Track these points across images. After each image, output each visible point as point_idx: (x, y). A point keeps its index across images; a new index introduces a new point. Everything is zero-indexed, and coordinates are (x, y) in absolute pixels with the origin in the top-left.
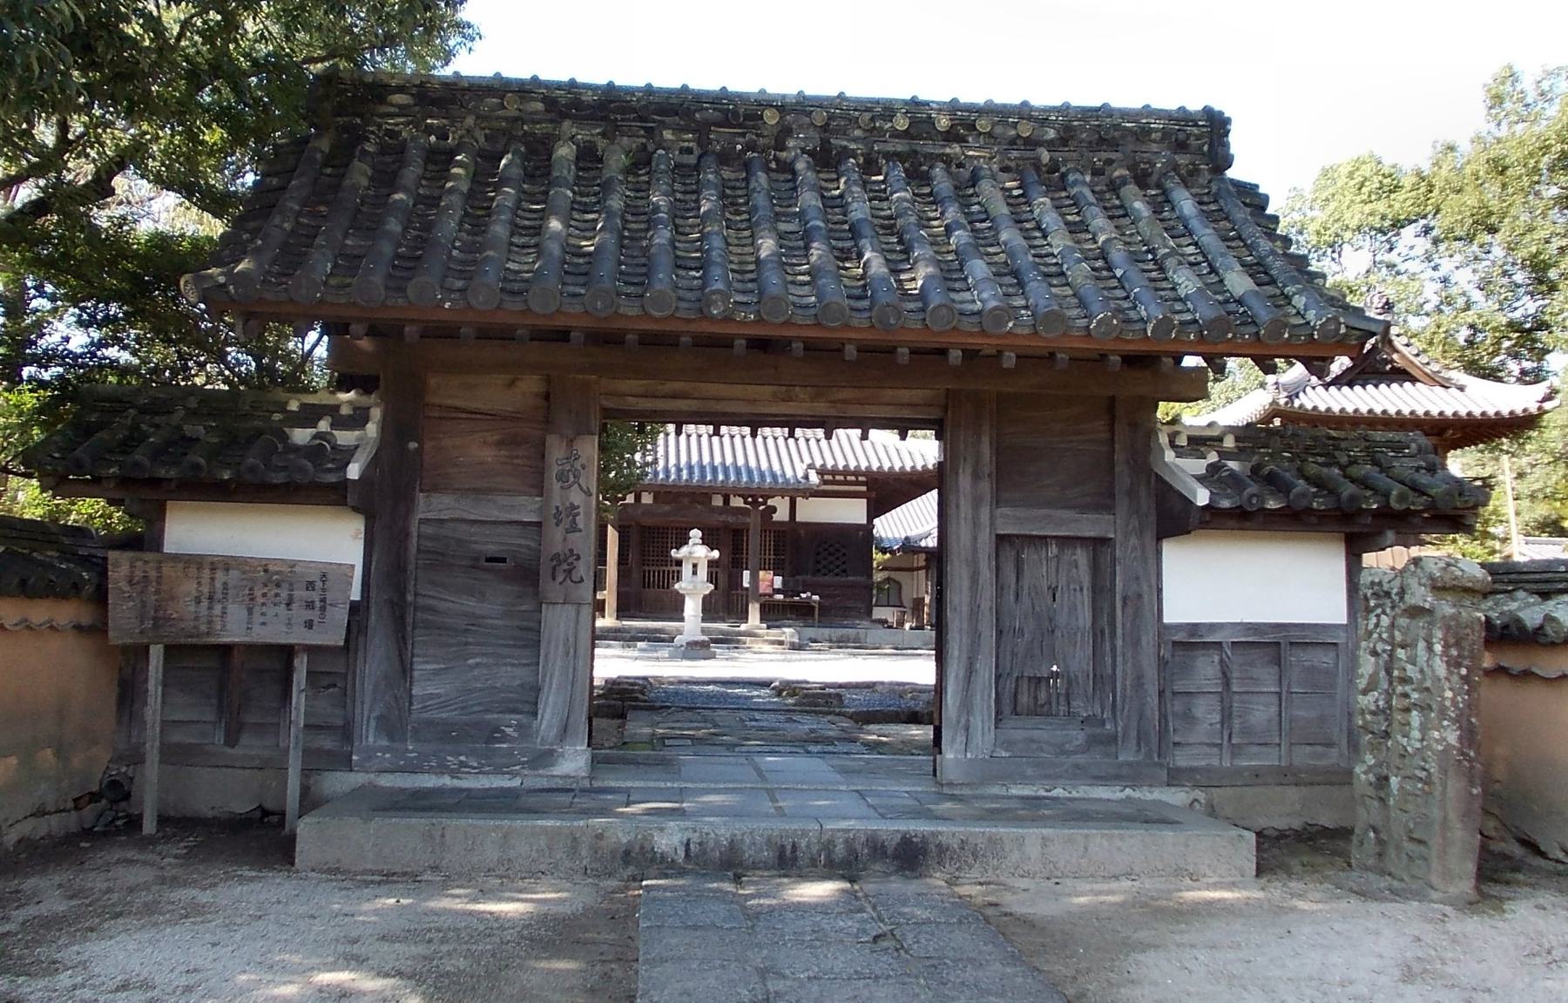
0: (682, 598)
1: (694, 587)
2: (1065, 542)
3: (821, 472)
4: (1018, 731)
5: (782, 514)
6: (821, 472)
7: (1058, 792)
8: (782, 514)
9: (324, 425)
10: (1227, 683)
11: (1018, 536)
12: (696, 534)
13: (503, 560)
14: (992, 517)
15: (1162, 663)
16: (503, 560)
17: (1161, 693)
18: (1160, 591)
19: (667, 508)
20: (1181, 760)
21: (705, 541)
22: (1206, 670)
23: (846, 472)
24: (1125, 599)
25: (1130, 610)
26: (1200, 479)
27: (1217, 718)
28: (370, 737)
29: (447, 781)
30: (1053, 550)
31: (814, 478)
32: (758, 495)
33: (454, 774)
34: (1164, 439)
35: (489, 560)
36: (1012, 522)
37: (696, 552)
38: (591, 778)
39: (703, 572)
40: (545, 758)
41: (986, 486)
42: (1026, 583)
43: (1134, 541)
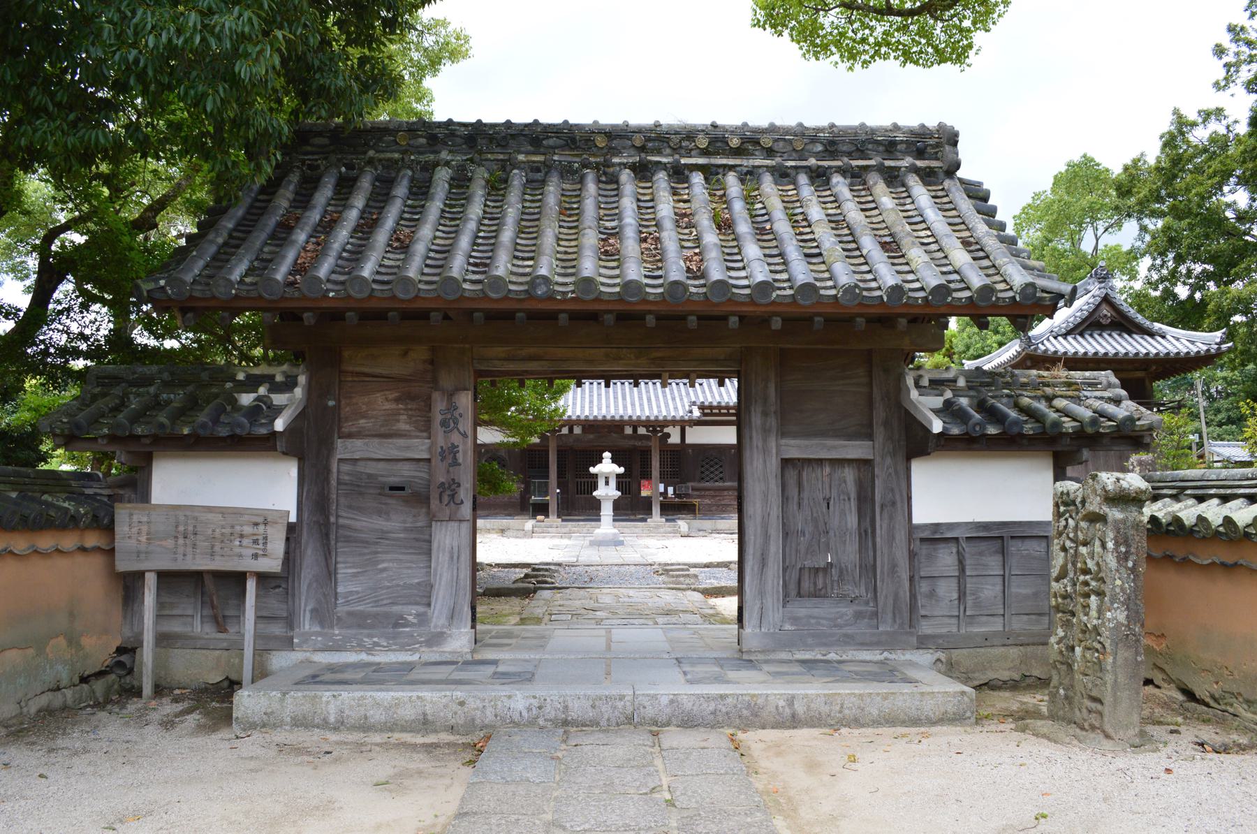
1: (607, 492)
2: (834, 462)
3: (702, 407)
5: (675, 439)
6: (702, 407)
7: (832, 656)
8: (675, 439)
9: (262, 390)
10: (962, 569)
11: (799, 459)
12: (607, 455)
13: (402, 489)
14: (778, 446)
15: (912, 555)
16: (402, 489)
17: (911, 579)
18: (909, 498)
19: (591, 436)
20: (926, 628)
21: (614, 460)
22: (946, 560)
23: (719, 407)
24: (882, 506)
25: (886, 515)
26: (937, 412)
27: (955, 596)
28: (307, 624)
29: (364, 657)
30: (827, 470)
31: (697, 413)
32: (657, 426)
33: (369, 651)
34: (910, 381)
35: (392, 488)
36: (796, 448)
37: (607, 467)
38: (473, 652)
39: (613, 483)
40: (436, 639)
41: (773, 422)
42: (805, 495)
43: (888, 461)
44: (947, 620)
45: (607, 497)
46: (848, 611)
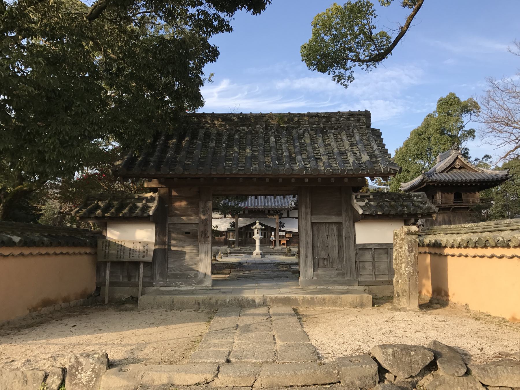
2: (329, 223)
7: (330, 287)
9: (144, 202)
10: (374, 259)
11: (318, 223)
13: (189, 233)
14: (311, 219)
15: (356, 254)
16: (189, 233)
17: (356, 262)
18: (355, 235)
20: (362, 279)
22: (368, 256)
24: (345, 238)
25: (347, 240)
26: (361, 207)
27: (371, 268)
28: (158, 278)
29: (177, 288)
30: (327, 226)
33: (178, 286)
34: (354, 197)
35: (186, 233)
38: (212, 286)
41: (309, 210)
42: (320, 234)
43: (347, 223)
44: (368, 276)
46: (335, 272)
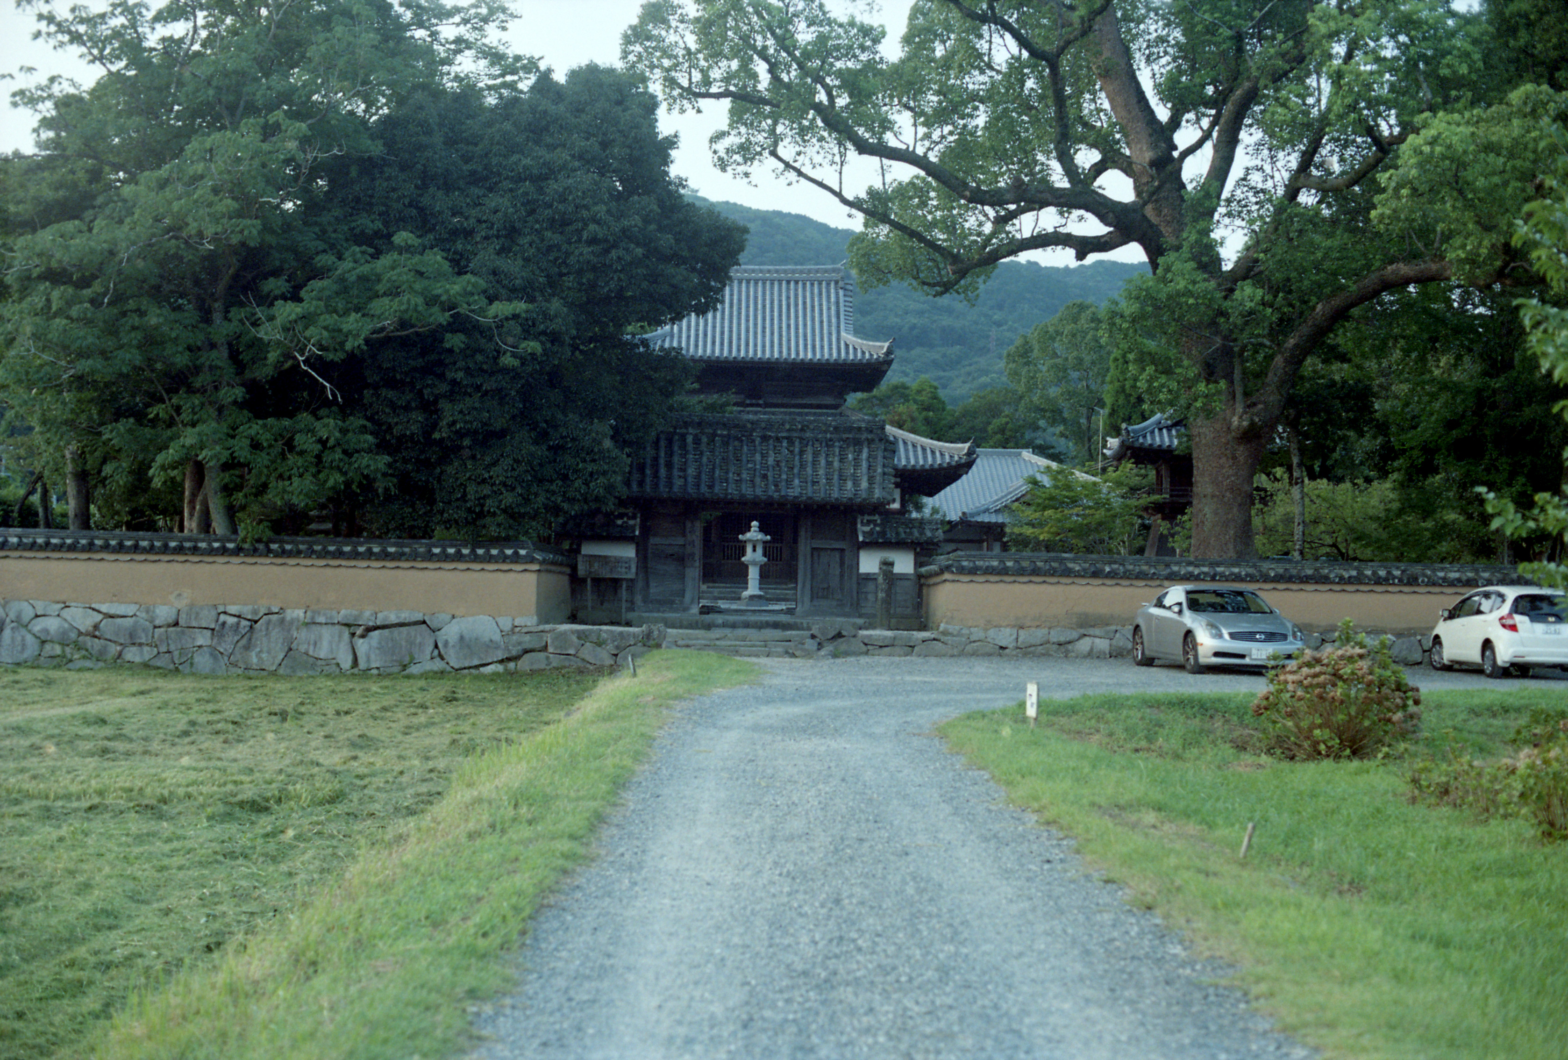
0: (747, 567)
1: (753, 557)
4: (815, 603)
12: (755, 523)
21: (762, 529)
36: (817, 544)
37: (754, 533)
39: (760, 550)
40: (685, 609)
45: (754, 563)
46: (834, 603)
